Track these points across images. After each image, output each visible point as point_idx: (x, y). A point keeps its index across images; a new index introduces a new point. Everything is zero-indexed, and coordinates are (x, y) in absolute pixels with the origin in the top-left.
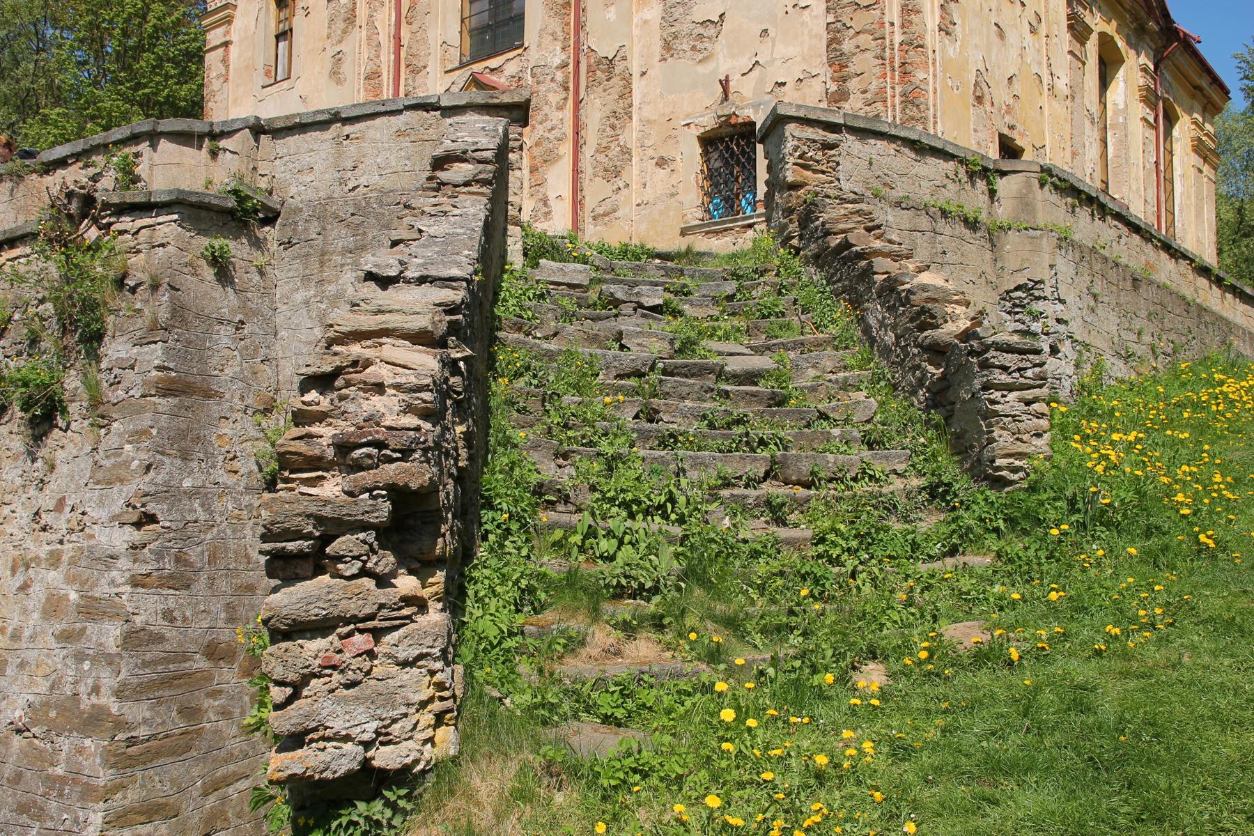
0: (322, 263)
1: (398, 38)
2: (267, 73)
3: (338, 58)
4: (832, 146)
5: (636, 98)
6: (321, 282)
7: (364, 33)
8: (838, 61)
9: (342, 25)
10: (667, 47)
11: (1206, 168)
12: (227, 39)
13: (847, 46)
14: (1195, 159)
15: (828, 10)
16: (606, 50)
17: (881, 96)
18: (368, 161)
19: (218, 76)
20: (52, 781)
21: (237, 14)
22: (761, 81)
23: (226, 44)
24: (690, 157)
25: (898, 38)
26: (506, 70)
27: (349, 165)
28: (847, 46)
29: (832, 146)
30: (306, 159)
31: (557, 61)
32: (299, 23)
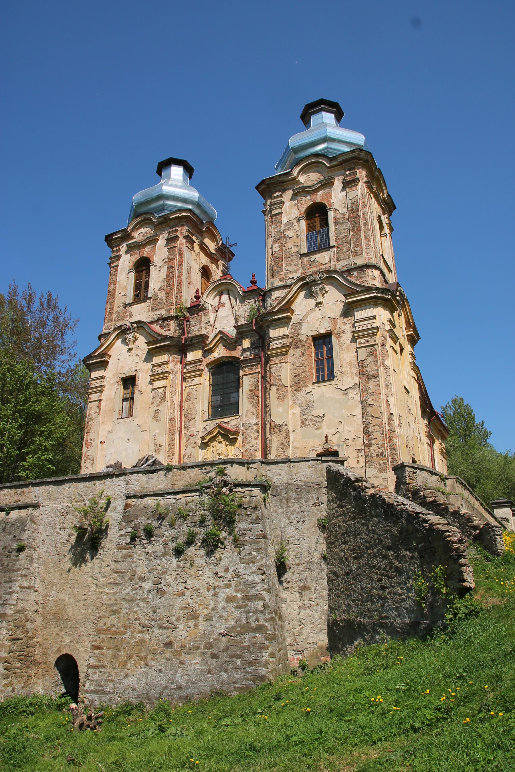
0: (287, 502)
1: (181, 406)
2: (119, 413)
3: (157, 412)
4: (414, 473)
5: (291, 439)
6: (287, 507)
7: (169, 404)
8: (367, 434)
9: (158, 400)
10: (303, 423)
11: (444, 460)
12: (100, 398)
13: (370, 429)
14: (441, 457)
15: (363, 417)
16: (278, 421)
17: (383, 446)
18: (300, 474)
19: (95, 413)
20: (244, 648)
21: (105, 389)
22: (340, 437)
23: (100, 400)
25: (387, 428)
26: (231, 423)
27: (294, 474)
28: (370, 429)
29: (414, 473)
30: (279, 472)
31: (254, 422)
32: (136, 395)
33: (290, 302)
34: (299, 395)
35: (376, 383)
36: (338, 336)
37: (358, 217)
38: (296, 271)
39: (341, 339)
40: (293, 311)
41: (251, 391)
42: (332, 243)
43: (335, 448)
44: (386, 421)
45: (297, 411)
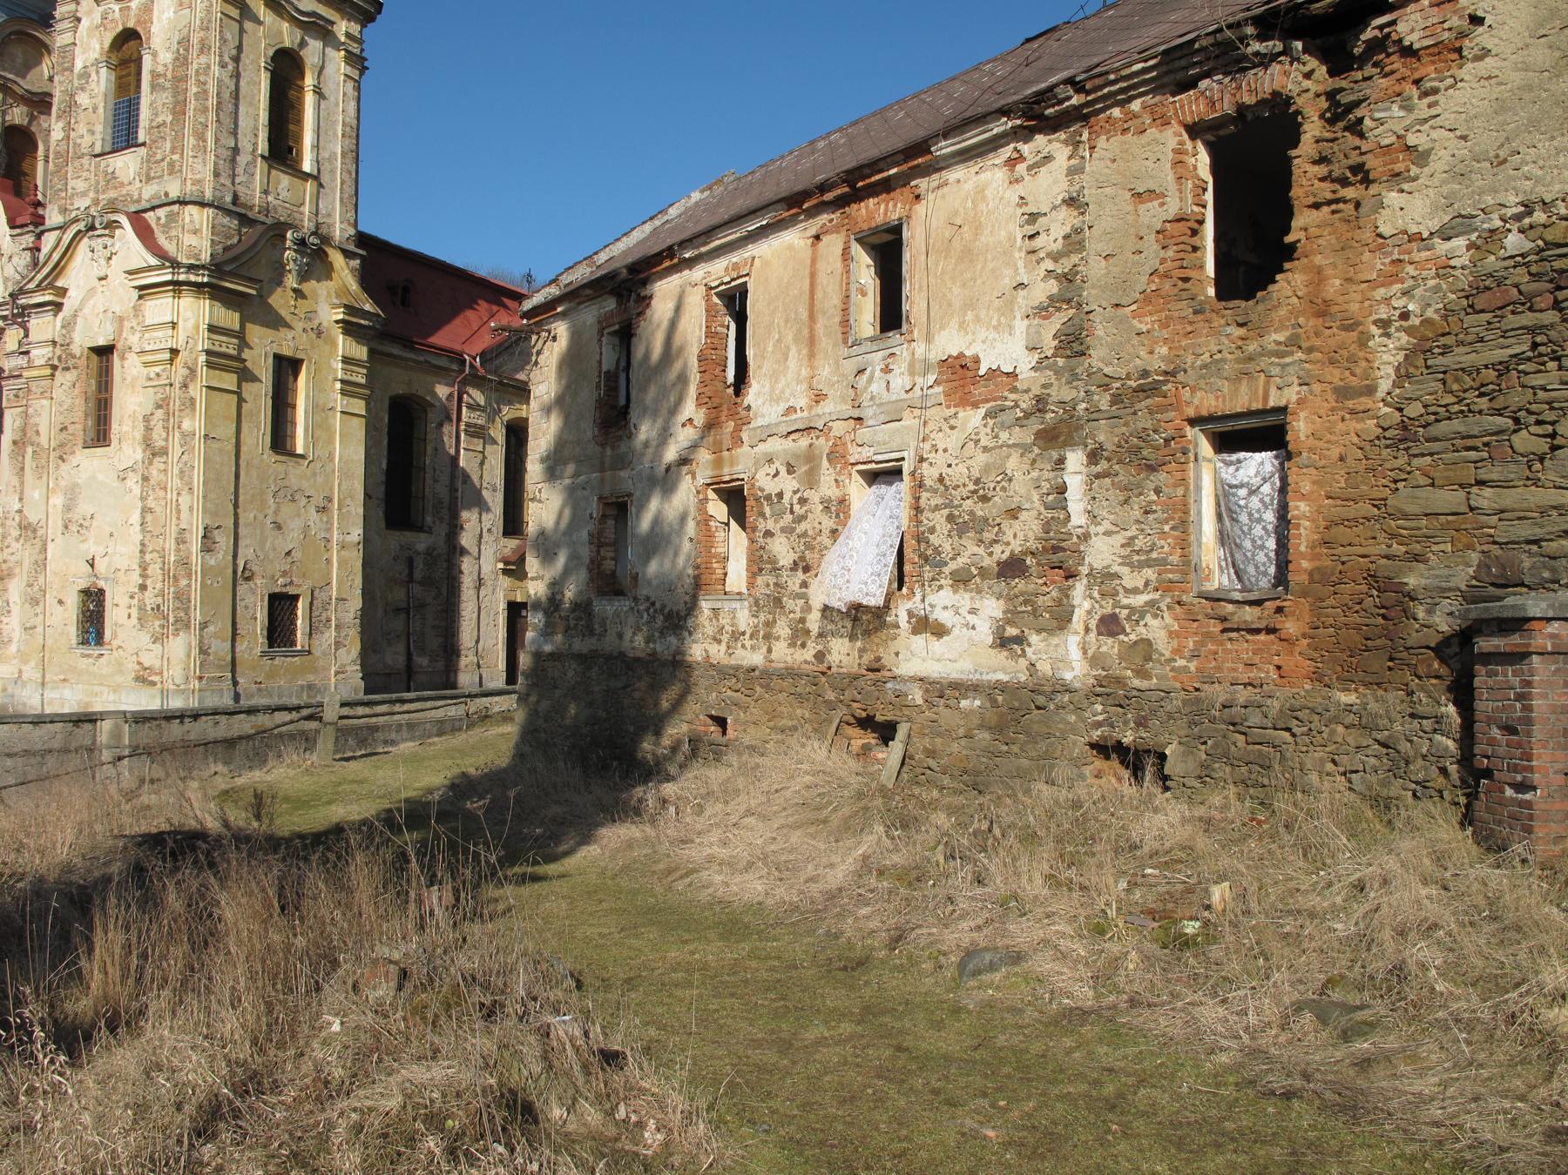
8: (144, 567)
22: (109, 564)
24: (73, 601)
28: (148, 557)
33: (59, 270)
34: (64, 467)
35: (162, 466)
36: (123, 358)
37: (185, 79)
38: (84, 194)
39: (126, 364)
40: (63, 292)
41: (15, 443)
42: (141, 137)
43: (101, 584)
44: (171, 544)
45: (58, 501)
